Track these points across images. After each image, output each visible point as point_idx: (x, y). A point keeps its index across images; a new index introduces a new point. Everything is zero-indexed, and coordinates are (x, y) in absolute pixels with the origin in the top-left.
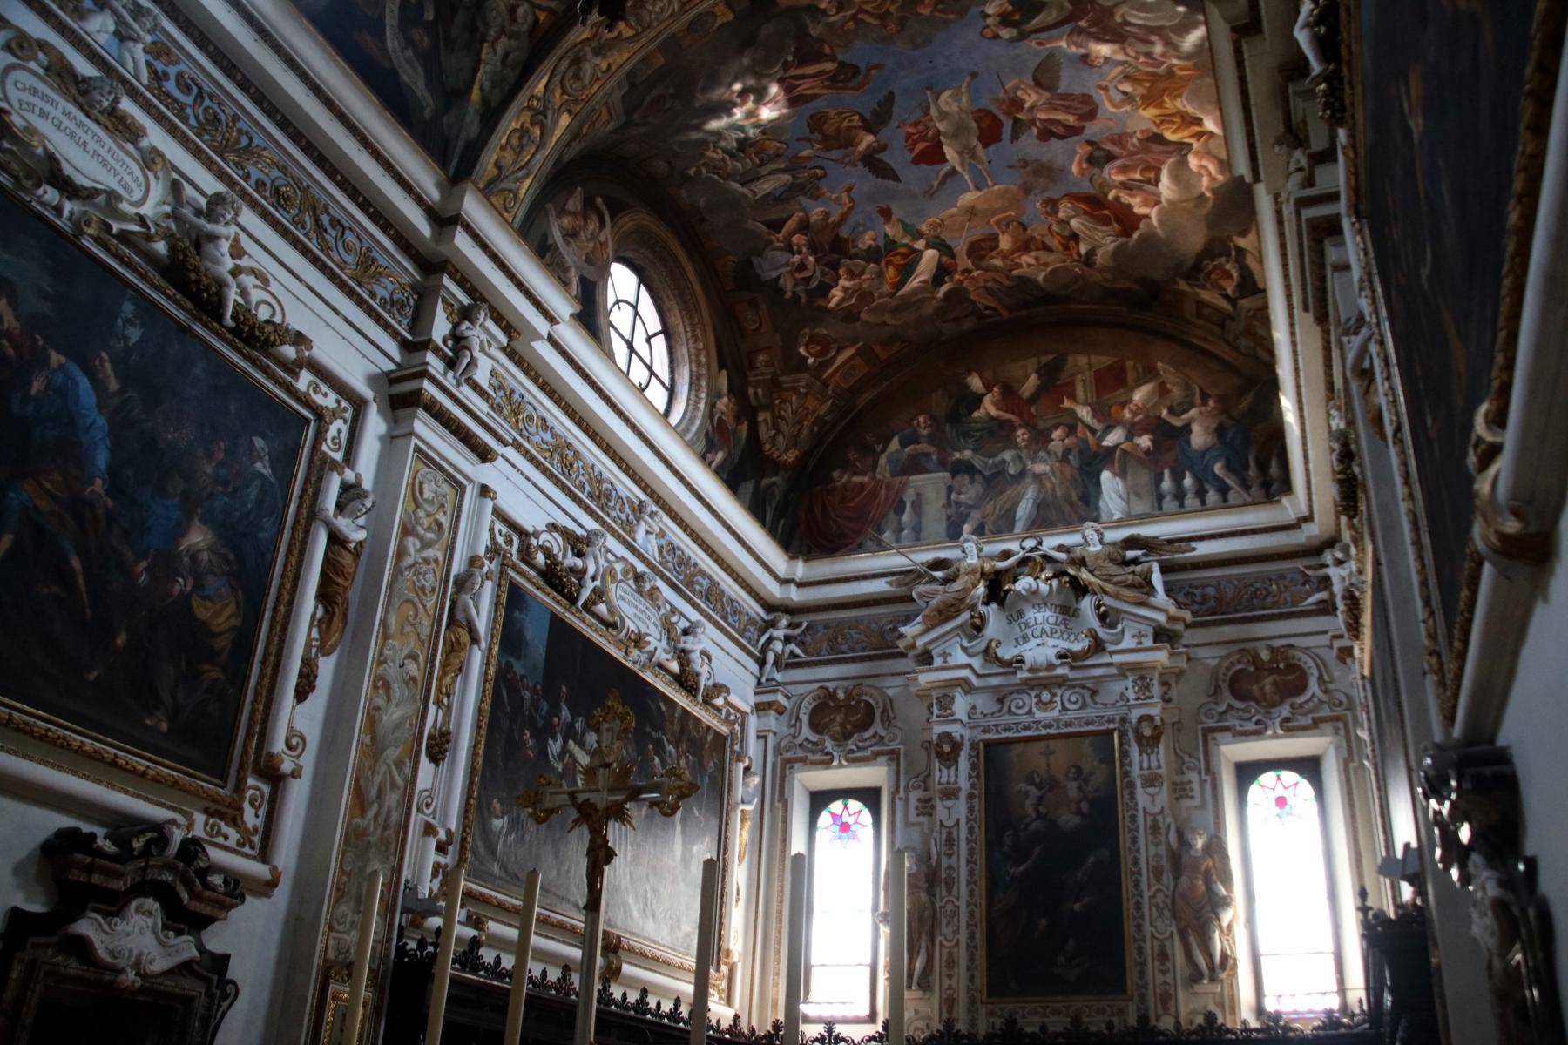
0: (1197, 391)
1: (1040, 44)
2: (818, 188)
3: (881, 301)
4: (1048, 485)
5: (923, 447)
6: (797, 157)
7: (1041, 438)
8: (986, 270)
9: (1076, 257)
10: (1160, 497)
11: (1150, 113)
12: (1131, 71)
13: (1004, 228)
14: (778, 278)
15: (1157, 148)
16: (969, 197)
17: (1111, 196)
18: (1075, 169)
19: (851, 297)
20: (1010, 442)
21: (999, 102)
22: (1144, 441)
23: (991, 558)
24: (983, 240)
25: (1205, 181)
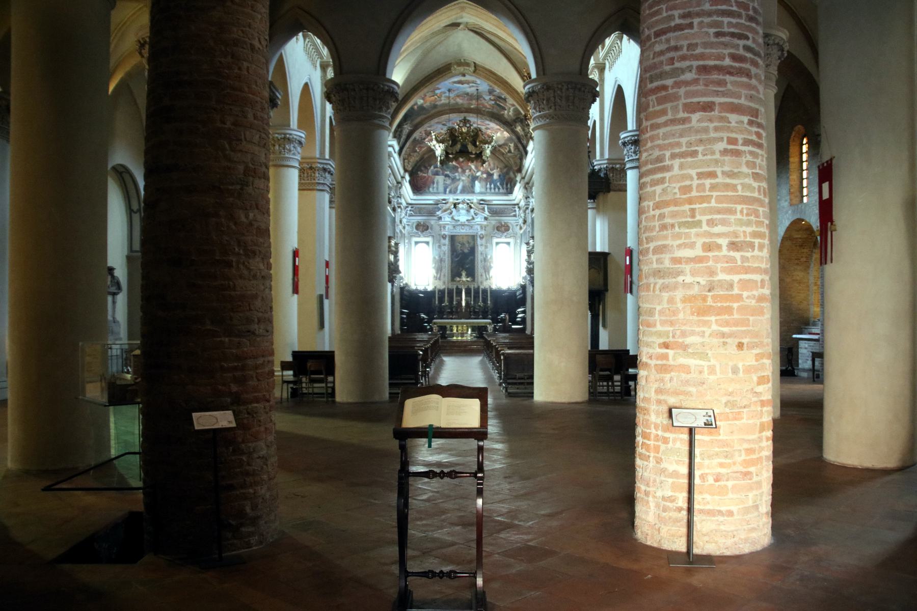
5: (439, 169)
7: (464, 171)
10: (487, 189)
20: (457, 171)
22: (485, 176)
23: (454, 199)
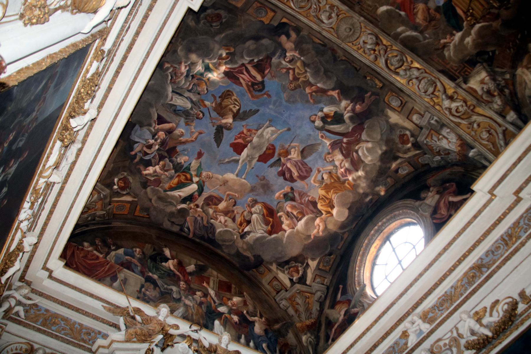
0: (259, 312)
1: (322, 137)
2: (193, 121)
3: (160, 189)
4: (190, 311)
6: (203, 101)
7: (191, 291)
8: (204, 211)
9: (240, 231)
11: (322, 192)
12: (334, 171)
13: (228, 199)
14: (137, 142)
15: (311, 207)
16: (230, 176)
17: (279, 214)
18: (277, 194)
19: (153, 176)
21: (283, 147)
22: (236, 318)
24: (215, 197)
25: (315, 231)
